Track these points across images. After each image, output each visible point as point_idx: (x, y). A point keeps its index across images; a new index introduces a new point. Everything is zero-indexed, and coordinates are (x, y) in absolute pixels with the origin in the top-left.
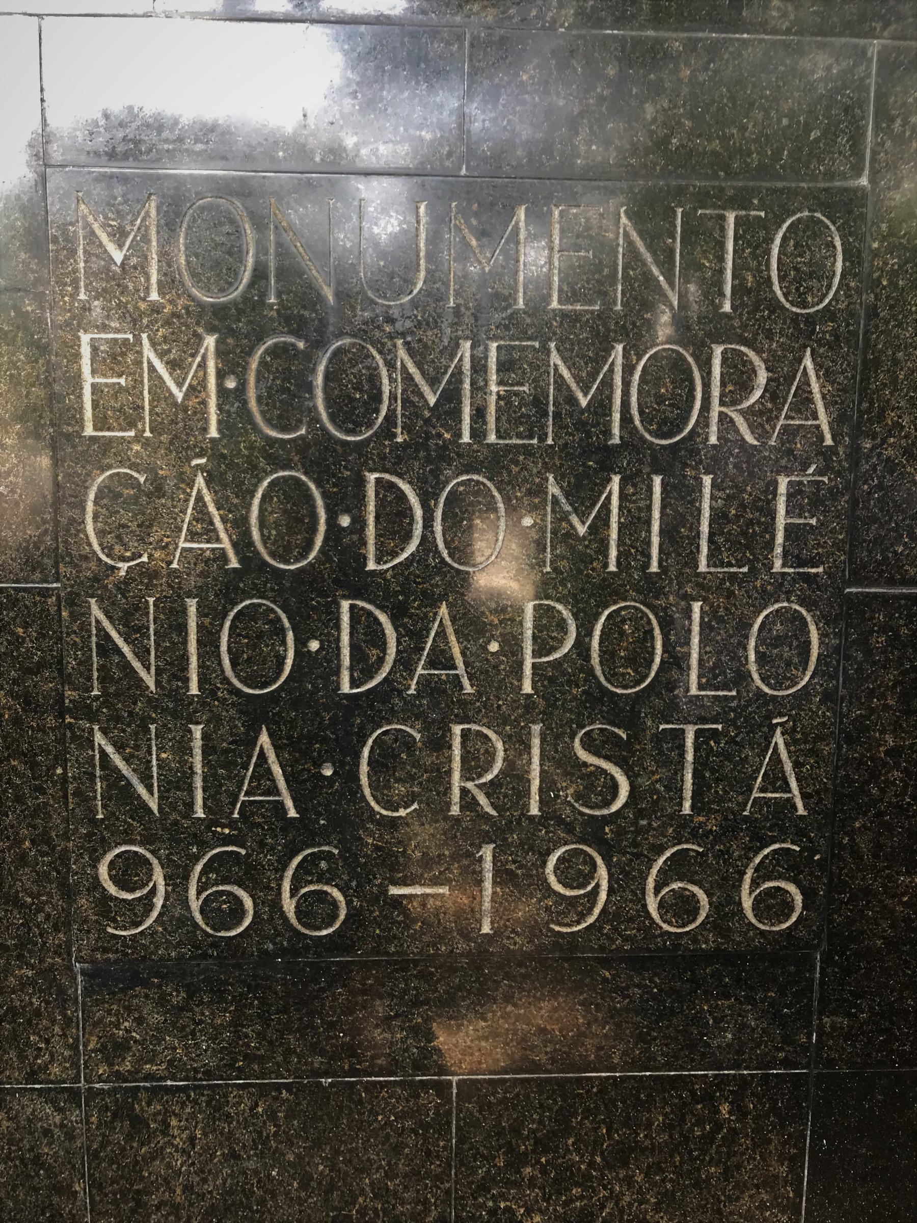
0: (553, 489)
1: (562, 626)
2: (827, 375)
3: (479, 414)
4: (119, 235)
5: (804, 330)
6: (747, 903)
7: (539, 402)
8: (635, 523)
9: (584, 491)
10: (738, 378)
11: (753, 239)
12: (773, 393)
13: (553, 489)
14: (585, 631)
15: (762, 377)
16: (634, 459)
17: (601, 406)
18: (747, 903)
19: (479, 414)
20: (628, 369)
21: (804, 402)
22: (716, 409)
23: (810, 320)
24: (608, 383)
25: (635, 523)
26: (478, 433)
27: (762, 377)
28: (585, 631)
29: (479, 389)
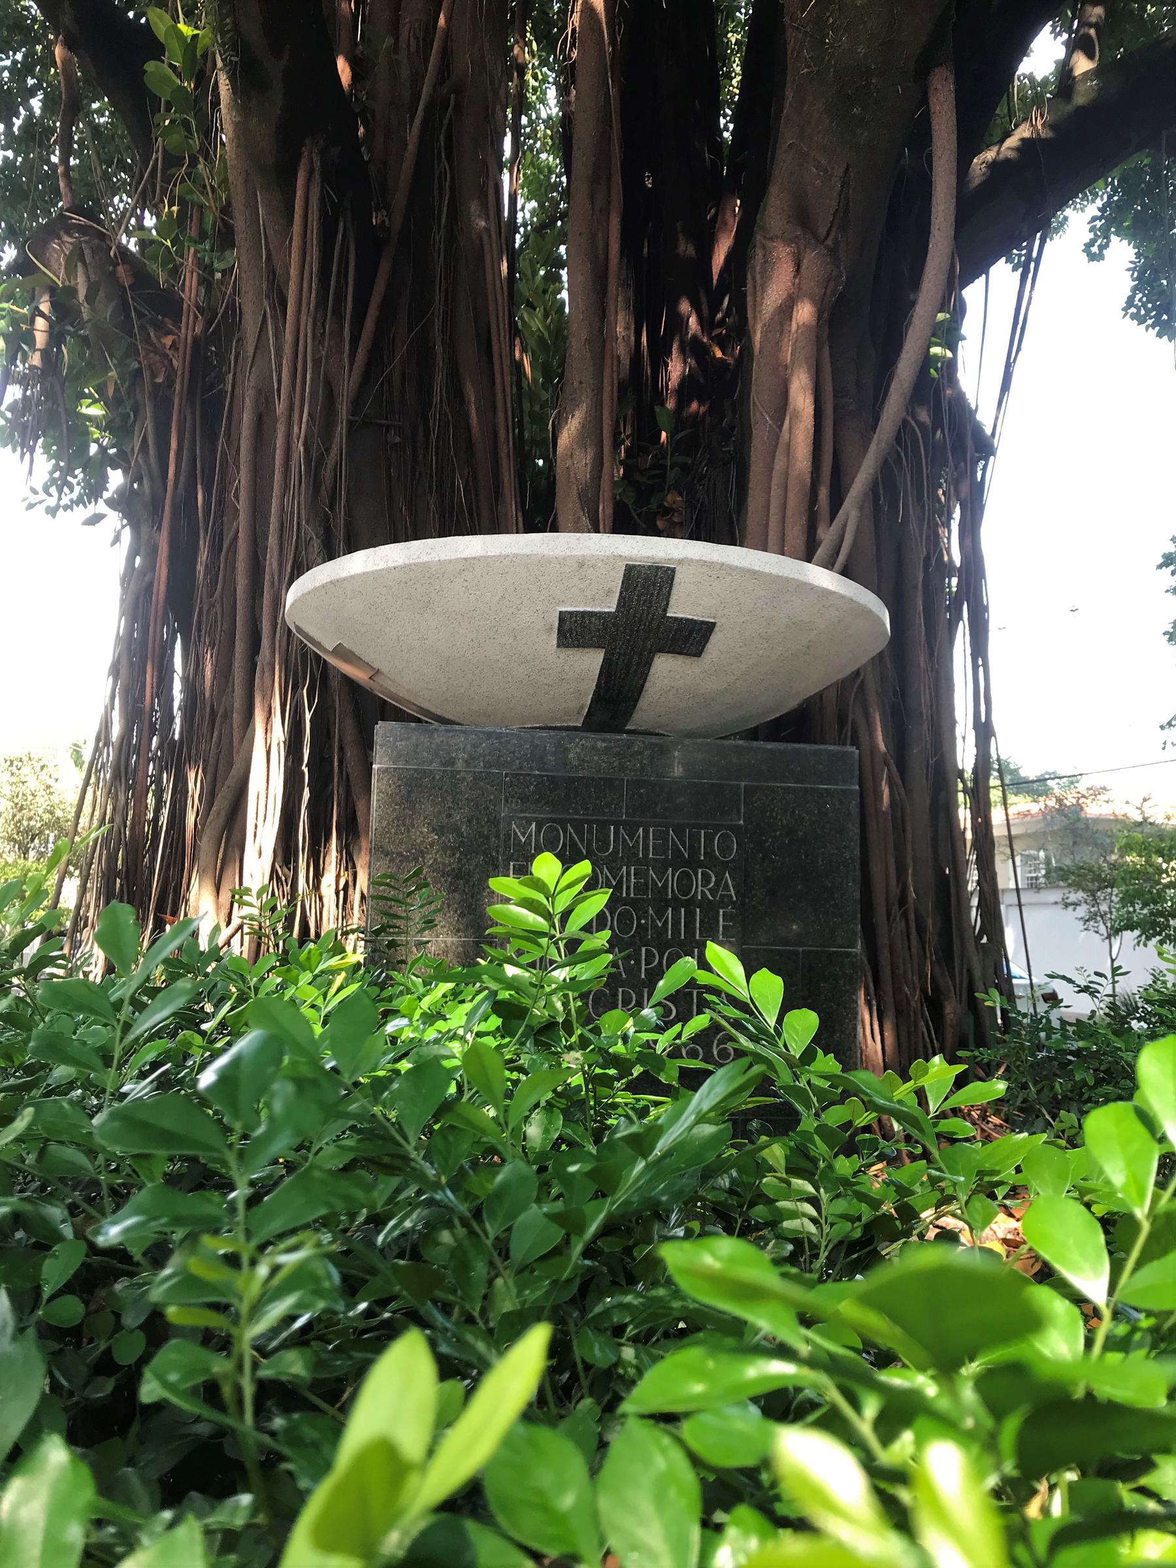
0: (651, 912)
1: (654, 956)
2: (733, 879)
3: (628, 888)
4: (523, 834)
5: (725, 866)
6: (715, 1053)
7: (646, 884)
8: (676, 923)
9: (660, 913)
10: (706, 879)
11: (709, 839)
12: (717, 883)
13: (651, 912)
14: (661, 958)
15: (713, 879)
16: (676, 904)
17: (665, 886)
18: (715, 1053)
19: (628, 888)
20: (673, 875)
21: (726, 887)
22: (700, 888)
23: (727, 862)
24: (667, 880)
25: (676, 923)
26: (628, 894)
27: (713, 879)
28: (661, 958)
29: (628, 880)
